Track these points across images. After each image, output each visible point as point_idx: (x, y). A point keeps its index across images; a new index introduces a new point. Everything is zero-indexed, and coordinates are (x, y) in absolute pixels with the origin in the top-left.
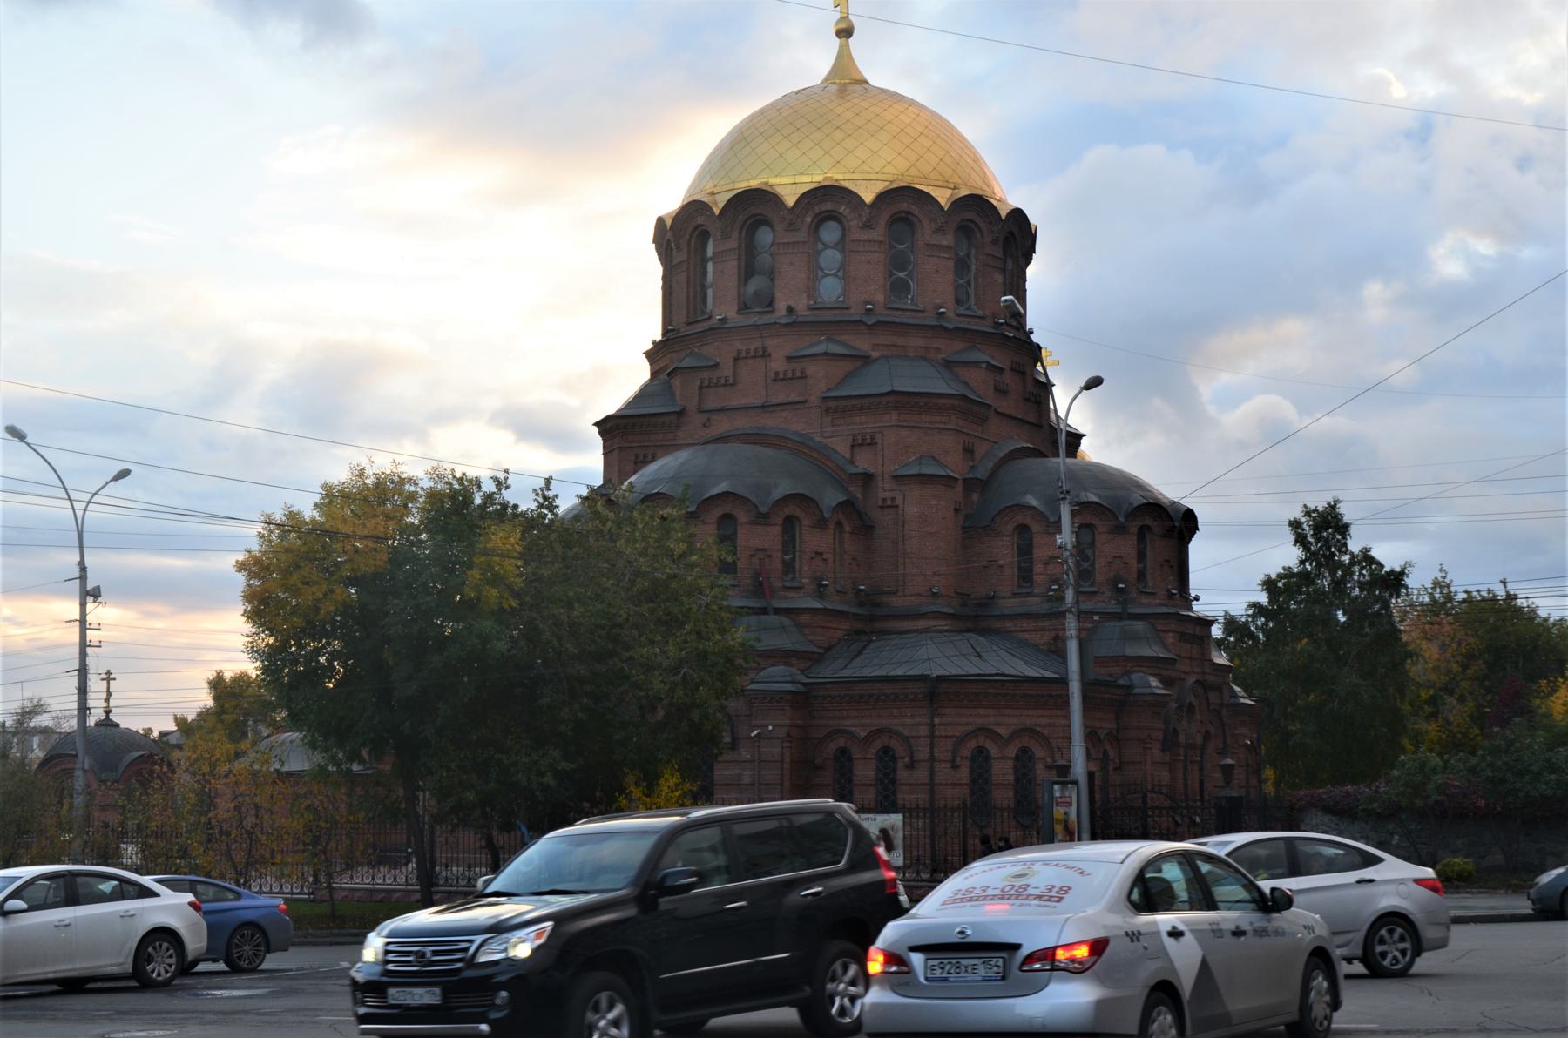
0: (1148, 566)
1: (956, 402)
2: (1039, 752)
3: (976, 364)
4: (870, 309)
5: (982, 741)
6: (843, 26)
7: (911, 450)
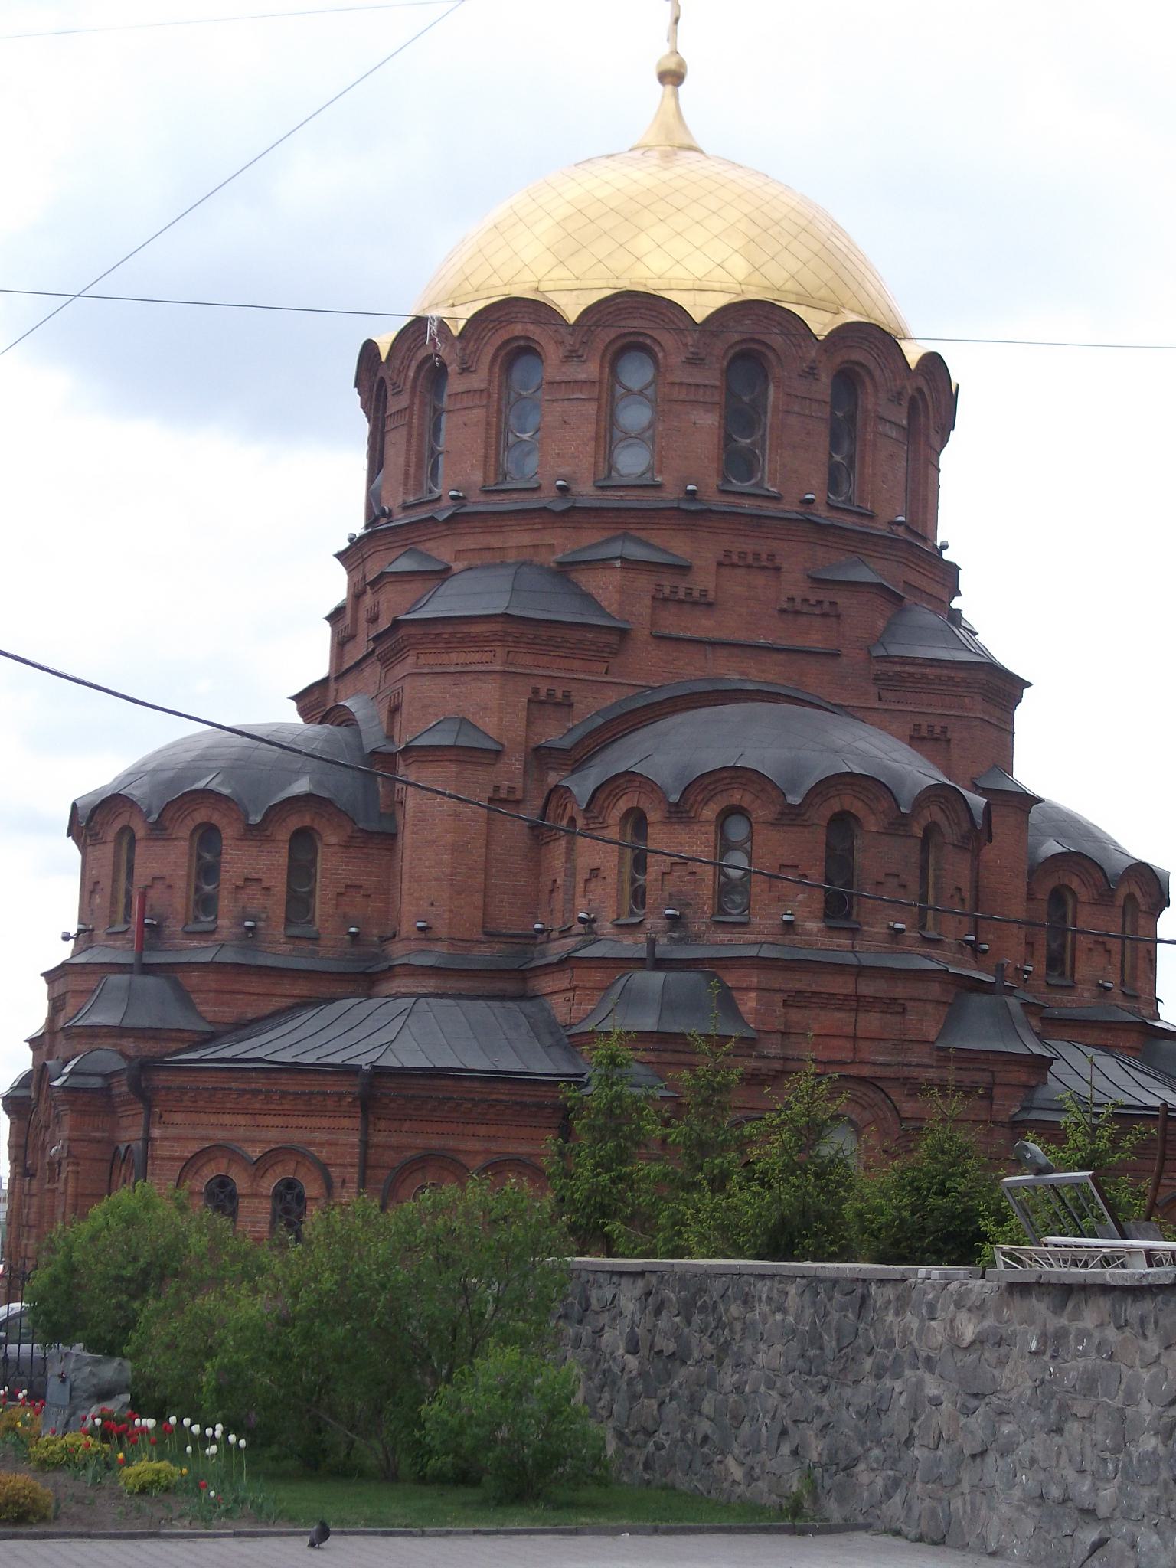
2: (312, 1189)
4: (693, 492)
6: (671, 64)
7: (431, 710)
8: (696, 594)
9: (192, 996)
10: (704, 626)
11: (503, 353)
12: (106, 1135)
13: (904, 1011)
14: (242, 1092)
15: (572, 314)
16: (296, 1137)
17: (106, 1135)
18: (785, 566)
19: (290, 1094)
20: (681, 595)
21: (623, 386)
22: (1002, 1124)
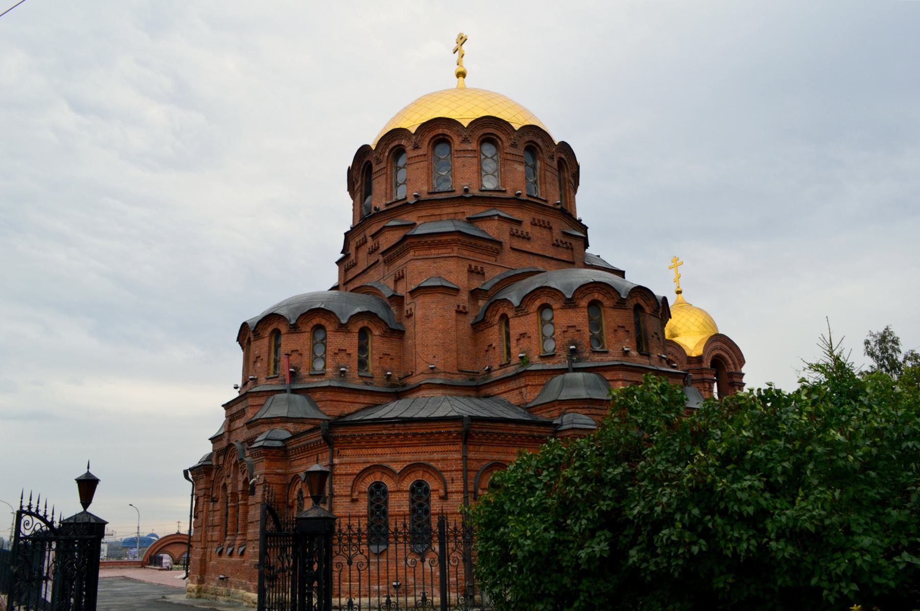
0: (604, 331)
1: (455, 237)
2: (433, 484)
3: (490, 218)
5: (377, 477)
7: (423, 274)
8: (525, 234)
9: (317, 404)
10: (527, 247)
11: (433, 141)
12: (283, 471)
14: (389, 436)
15: (465, 124)
16: (423, 457)
17: (283, 471)
18: (553, 227)
19: (419, 434)
20: (520, 233)
21: (484, 155)
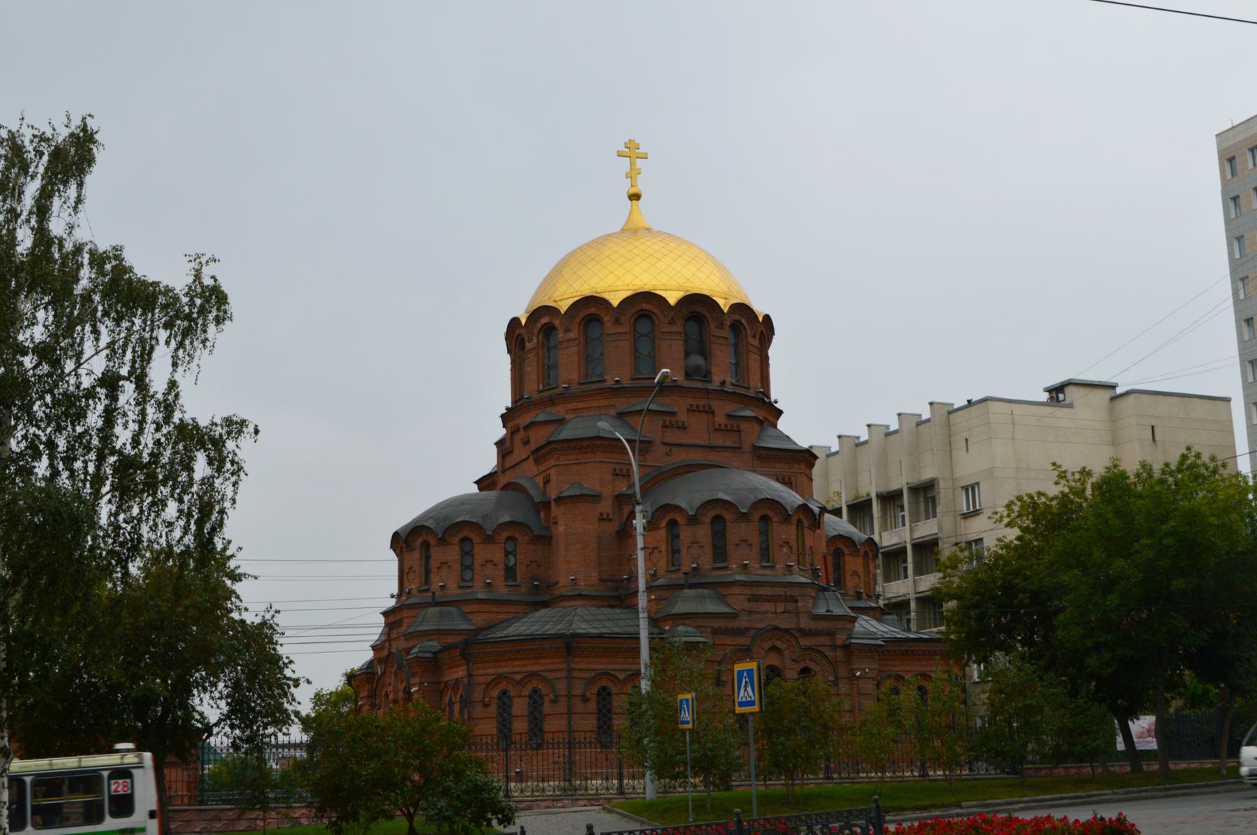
13: (797, 601)
22: (839, 647)
